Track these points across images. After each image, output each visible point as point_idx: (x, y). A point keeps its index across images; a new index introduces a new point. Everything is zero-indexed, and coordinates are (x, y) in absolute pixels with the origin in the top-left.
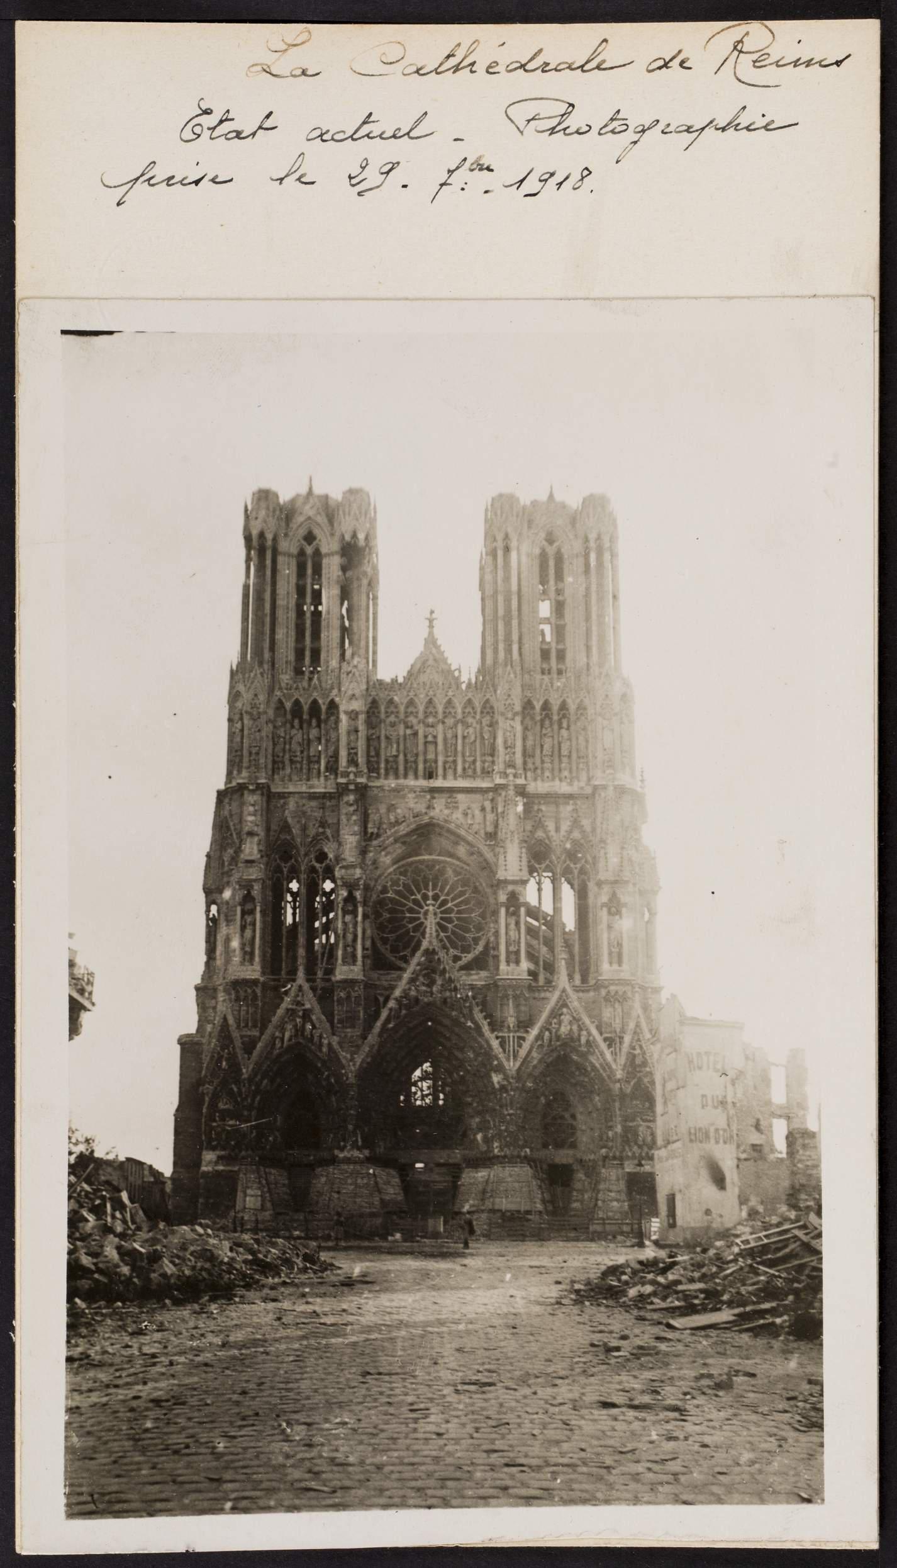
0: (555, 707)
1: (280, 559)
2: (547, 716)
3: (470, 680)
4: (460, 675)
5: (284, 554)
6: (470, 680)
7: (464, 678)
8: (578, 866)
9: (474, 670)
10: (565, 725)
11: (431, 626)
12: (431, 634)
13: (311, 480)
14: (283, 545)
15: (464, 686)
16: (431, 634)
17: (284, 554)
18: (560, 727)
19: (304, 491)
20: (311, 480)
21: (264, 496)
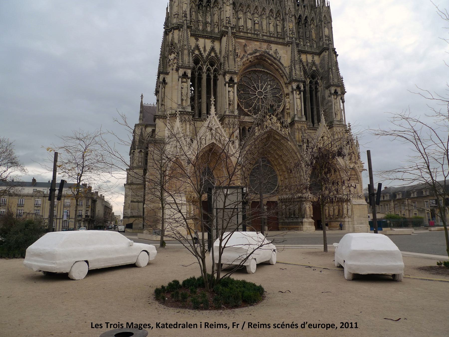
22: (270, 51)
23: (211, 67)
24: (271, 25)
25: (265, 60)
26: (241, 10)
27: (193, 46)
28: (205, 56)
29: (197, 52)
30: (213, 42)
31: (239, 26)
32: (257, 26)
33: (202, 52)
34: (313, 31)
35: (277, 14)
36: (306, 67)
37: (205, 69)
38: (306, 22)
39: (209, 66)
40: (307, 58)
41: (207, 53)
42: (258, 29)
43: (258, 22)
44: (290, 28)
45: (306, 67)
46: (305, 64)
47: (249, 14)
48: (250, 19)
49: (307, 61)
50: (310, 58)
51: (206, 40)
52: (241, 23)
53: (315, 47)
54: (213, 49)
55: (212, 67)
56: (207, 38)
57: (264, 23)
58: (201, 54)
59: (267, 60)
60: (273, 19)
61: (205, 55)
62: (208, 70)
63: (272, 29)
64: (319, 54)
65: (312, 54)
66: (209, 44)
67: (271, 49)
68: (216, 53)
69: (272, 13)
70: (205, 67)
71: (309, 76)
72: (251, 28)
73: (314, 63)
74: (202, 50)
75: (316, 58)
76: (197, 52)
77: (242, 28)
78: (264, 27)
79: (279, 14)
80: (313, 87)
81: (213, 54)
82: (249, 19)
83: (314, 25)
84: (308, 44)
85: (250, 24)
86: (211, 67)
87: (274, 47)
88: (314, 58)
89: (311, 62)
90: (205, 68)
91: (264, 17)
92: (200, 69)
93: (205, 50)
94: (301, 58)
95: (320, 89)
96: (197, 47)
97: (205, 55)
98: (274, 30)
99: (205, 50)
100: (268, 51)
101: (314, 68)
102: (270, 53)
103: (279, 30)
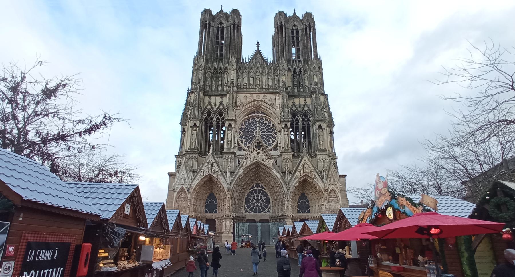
0: (297, 70)
1: (211, 28)
2: (295, 73)
3: (270, 62)
4: (267, 61)
5: (212, 26)
6: (270, 62)
7: (269, 62)
8: (307, 118)
9: (272, 59)
10: (301, 75)
11: (258, 47)
12: (258, 49)
13: (222, 7)
14: (212, 24)
15: (268, 64)
16: (258, 49)
17: (212, 26)
18: (299, 76)
19: (219, 11)
20: (222, 7)
21: (207, 12)
22: (266, 99)
23: (220, 117)
24: (270, 79)
25: (261, 107)
26: (245, 71)
27: (207, 102)
28: (215, 109)
29: (209, 107)
30: (222, 98)
31: (243, 84)
32: (258, 82)
33: (214, 106)
34: (306, 80)
35: (275, 70)
36: (299, 108)
37: (215, 118)
38: (300, 73)
39: (218, 116)
40: (299, 101)
41: (217, 106)
42: (259, 84)
43: (259, 79)
44: (283, 80)
45: (299, 108)
46: (298, 106)
47: (251, 74)
48: (253, 78)
49: (300, 103)
50: (302, 100)
51: (217, 97)
52: (245, 81)
53: (308, 91)
54: (221, 103)
55: (221, 116)
56: (218, 96)
57: (264, 79)
58: (212, 108)
59: (263, 107)
60: (272, 74)
61: (215, 108)
62: (218, 119)
63: (270, 82)
64: (310, 97)
65: (304, 97)
66: (219, 99)
67: (267, 98)
68: (223, 106)
69: (271, 70)
70: (215, 117)
71: (301, 115)
72: (253, 84)
73: (305, 104)
74: (213, 105)
75: (309, 101)
76: (209, 107)
77: (246, 85)
78: (264, 82)
79: (277, 70)
80: (306, 124)
81: (221, 107)
82: (251, 77)
83: (308, 74)
84: (302, 90)
85: (252, 81)
86: (220, 117)
87: (269, 96)
88: (306, 100)
89: (303, 103)
90: (215, 118)
91: (264, 75)
92: (212, 119)
93: (215, 105)
94: (294, 101)
95: (311, 124)
96: (210, 103)
97: (215, 108)
98: (272, 83)
99: (215, 105)
100: (263, 100)
101: (306, 108)
102: (266, 102)
103: (276, 82)
